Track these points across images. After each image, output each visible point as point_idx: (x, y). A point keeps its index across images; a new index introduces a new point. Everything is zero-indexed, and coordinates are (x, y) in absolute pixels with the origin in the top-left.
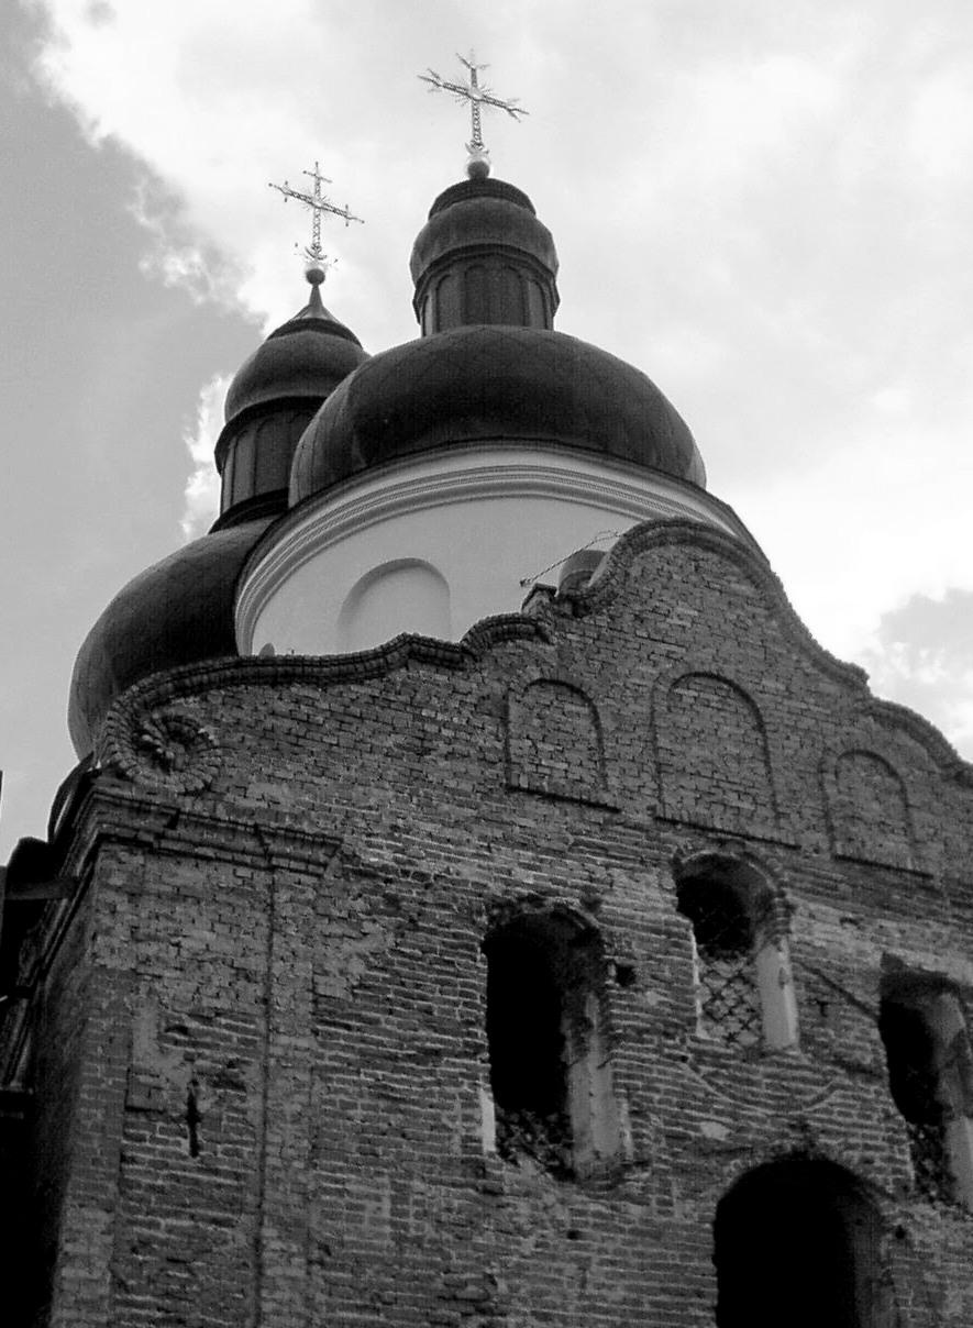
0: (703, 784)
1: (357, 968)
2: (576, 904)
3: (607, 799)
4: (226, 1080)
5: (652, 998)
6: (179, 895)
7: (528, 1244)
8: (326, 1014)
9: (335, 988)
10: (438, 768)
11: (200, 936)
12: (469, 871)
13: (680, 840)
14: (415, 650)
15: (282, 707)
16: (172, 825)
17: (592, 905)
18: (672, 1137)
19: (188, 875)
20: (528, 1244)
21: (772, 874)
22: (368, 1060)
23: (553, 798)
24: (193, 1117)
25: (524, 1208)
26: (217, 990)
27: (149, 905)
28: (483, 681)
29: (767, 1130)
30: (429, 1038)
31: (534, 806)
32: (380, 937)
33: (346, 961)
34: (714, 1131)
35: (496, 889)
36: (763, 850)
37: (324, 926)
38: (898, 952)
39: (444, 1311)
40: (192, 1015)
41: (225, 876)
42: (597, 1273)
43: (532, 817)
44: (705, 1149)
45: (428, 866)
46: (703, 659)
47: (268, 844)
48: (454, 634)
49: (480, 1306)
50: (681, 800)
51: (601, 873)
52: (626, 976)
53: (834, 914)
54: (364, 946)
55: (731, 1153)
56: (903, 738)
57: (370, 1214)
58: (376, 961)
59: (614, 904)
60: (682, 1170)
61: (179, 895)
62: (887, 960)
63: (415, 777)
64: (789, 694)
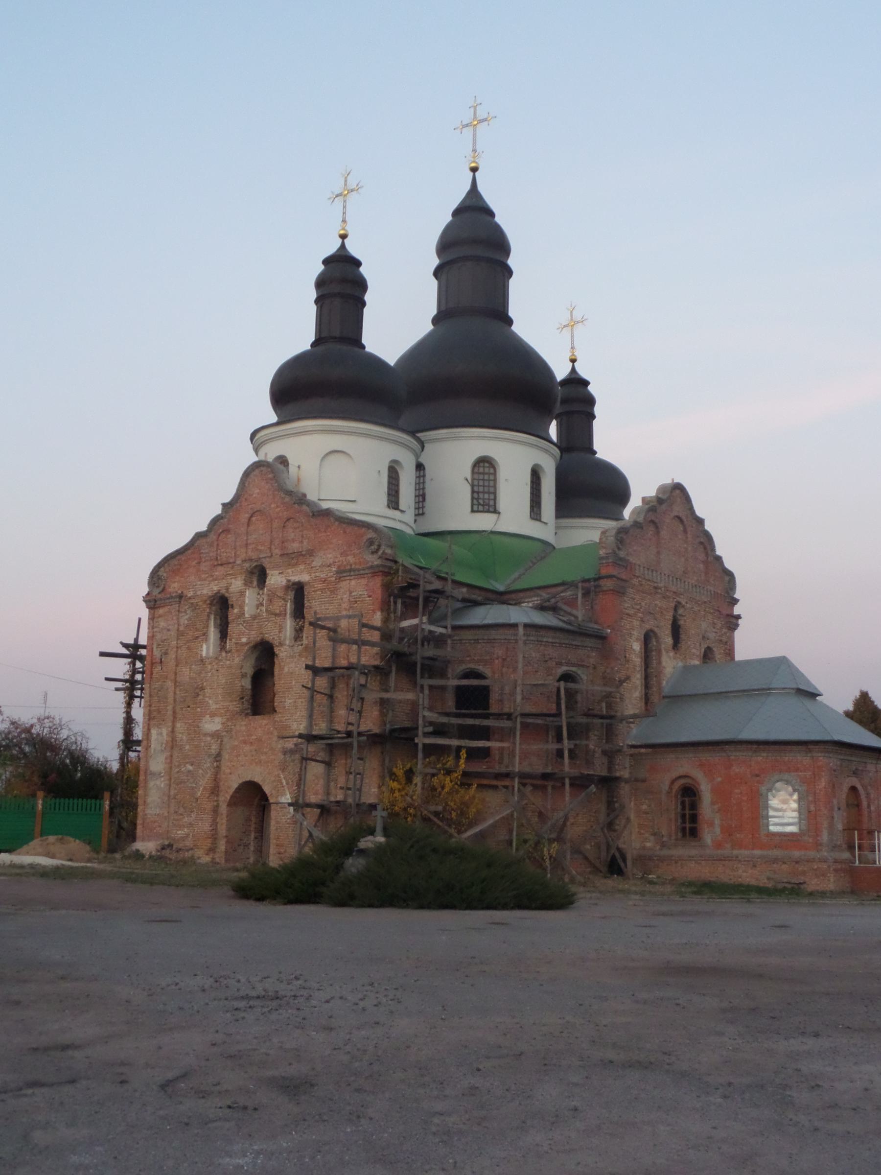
0: (253, 546)
1: (186, 622)
2: (223, 591)
3: (231, 561)
5: (236, 611)
6: (160, 616)
7: (210, 674)
9: (181, 628)
10: (204, 567)
11: (162, 624)
12: (205, 592)
13: (247, 565)
14: (199, 536)
15: (176, 563)
16: (156, 601)
17: (227, 589)
18: (236, 644)
19: (161, 611)
20: (210, 674)
22: (188, 642)
23: (222, 565)
24: (161, 662)
25: (209, 667)
27: (155, 620)
28: (213, 537)
30: (197, 634)
31: (220, 568)
33: (184, 620)
34: (244, 640)
35: (210, 594)
36: (264, 560)
37: (181, 615)
38: (290, 578)
39: (197, 691)
40: (163, 641)
41: (166, 609)
42: (220, 678)
43: (220, 571)
45: (199, 593)
48: (204, 528)
51: (230, 581)
52: (232, 606)
53: (277, 572)
54: (187, 617)
55: (247, 644)
57: (186, 674)
58: (189, 619)
59: (231, 589)
60: (237, 651)
62: (289, 581)
64: (277, 507)
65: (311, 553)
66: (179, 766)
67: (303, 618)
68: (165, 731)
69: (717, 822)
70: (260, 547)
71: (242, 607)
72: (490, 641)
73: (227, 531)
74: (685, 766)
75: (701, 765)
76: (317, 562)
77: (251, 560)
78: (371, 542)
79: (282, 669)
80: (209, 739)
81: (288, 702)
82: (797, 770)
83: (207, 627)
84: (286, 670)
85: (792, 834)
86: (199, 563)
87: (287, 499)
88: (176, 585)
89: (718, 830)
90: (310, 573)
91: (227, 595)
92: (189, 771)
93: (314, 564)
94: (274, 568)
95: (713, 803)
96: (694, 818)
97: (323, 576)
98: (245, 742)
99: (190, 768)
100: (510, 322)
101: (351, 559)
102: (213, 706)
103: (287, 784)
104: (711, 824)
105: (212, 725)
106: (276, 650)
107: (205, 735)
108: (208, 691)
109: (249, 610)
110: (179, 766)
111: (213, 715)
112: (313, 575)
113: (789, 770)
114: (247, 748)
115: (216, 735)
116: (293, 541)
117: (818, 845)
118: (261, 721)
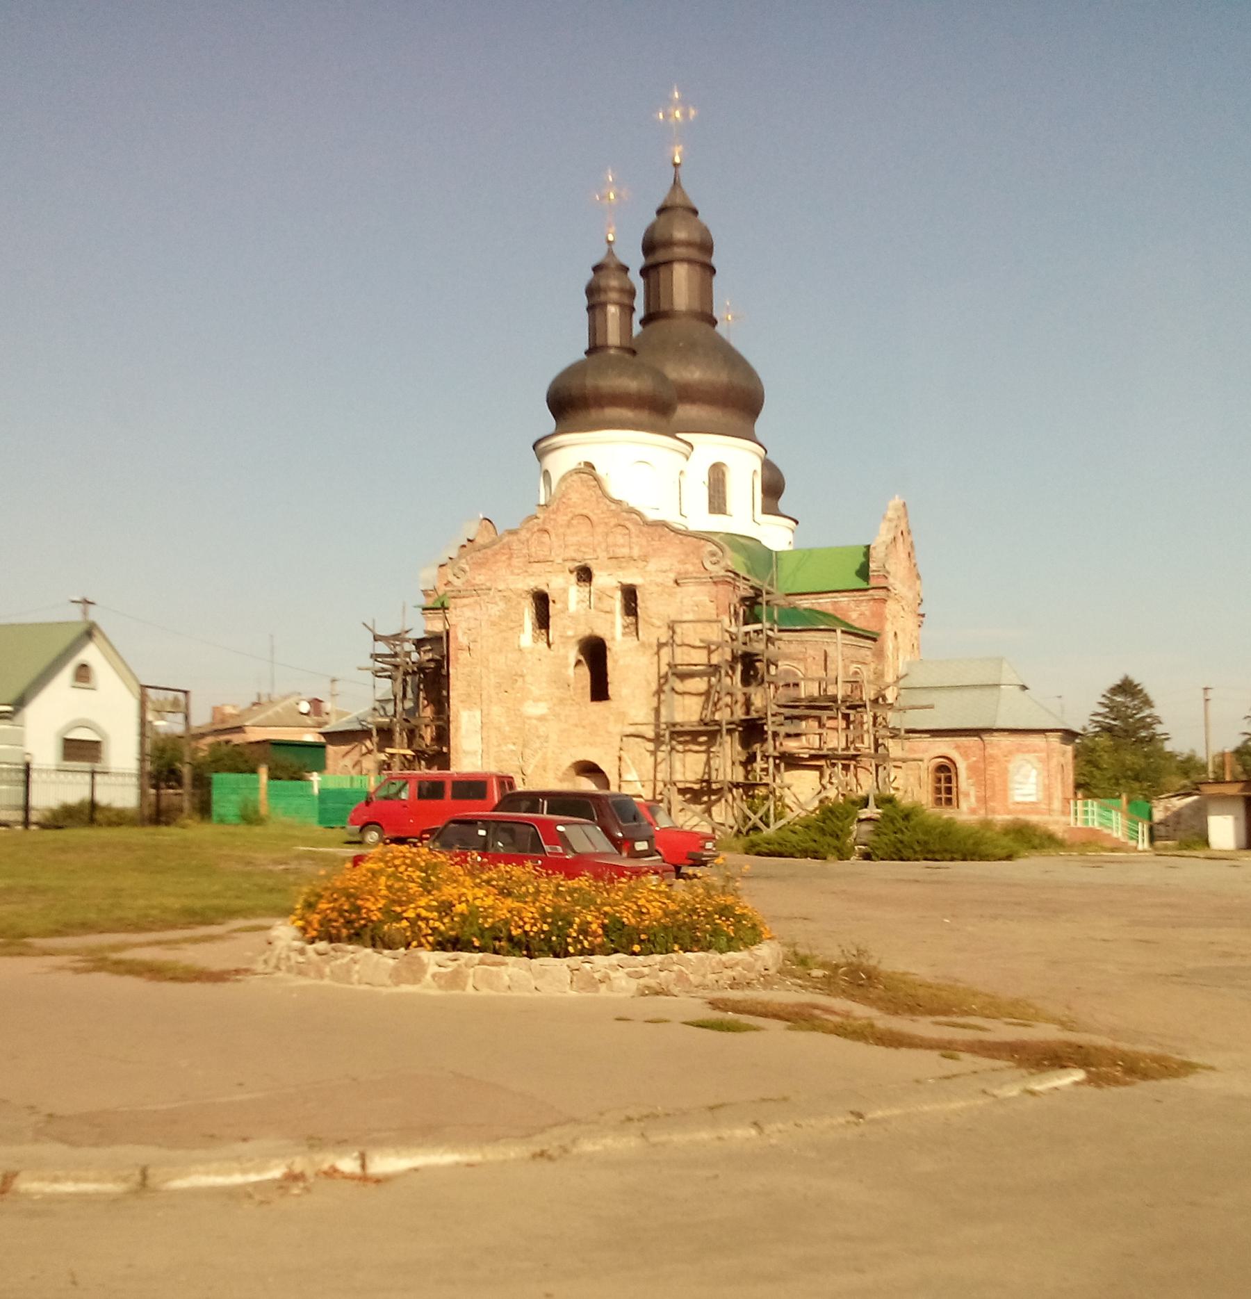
4: (475, 641)
5: (559, 606)
6: (465, 606)
8: (494, 624)
10: (515, 562)
19: (465, 601)
21: (593, 565)
22: (501, 631)
26: (473, 624)
29: (584, 631)
30: (512, 625)
32: (502, 605)
33: (495, 610)
34: (570, 633)
41: (471, 600)
44: (568, 638)
45: (512, 587)
46: (579, 511)
47: (477, 591)
49: (522, 676)
50: (571, 553)
56: (634, 516)
61: (465, 606)
63: (510, 565)
65: (645, 558)
66: (499, 745)
67: (635, 614)
68: (478, 714)
69: (972, 792)
70: (583, 549)
71: (566, 603)
72: (802, 642)
73: (546, 531)
74: (944, 747)
75: (957, 747)
76: (653, 566)
77: (574, 560)
78: (713, 554)
79: (616, 661)
80: (534, 722)
81: (625, 692)
82: (1035, 751)
83: (522, 619)
84: (621, 662)
85: (1033, 803)
86: (510, 558)
87: (613, 507)
88: (482, 577)
89: (973, 799)
90: (643, 576)
91: (547, 590)
92: (512, 751)
93: (648, 569)
94: (601, 569)
95: (969, 778)
96: (949, 790)
97: (659, 580)
98: (576, 726)
99: (513, 747)
100: (713, 322)
101: (690, 568)
102: (536, 691)
103: (633, 763)
104: (967, 795)
105: (534, 709)
106: (608, 644)
107: (529, 718)
108: (529, 679)
109: (573, 607)
110: (499, 745)
111: (537, 700)
112: (648, 579)
113: (1028, 752)
114: (580, 731)
115: (542, 719)
116: (623, 546)
117: (1050, 811)
118: (599, 706)
